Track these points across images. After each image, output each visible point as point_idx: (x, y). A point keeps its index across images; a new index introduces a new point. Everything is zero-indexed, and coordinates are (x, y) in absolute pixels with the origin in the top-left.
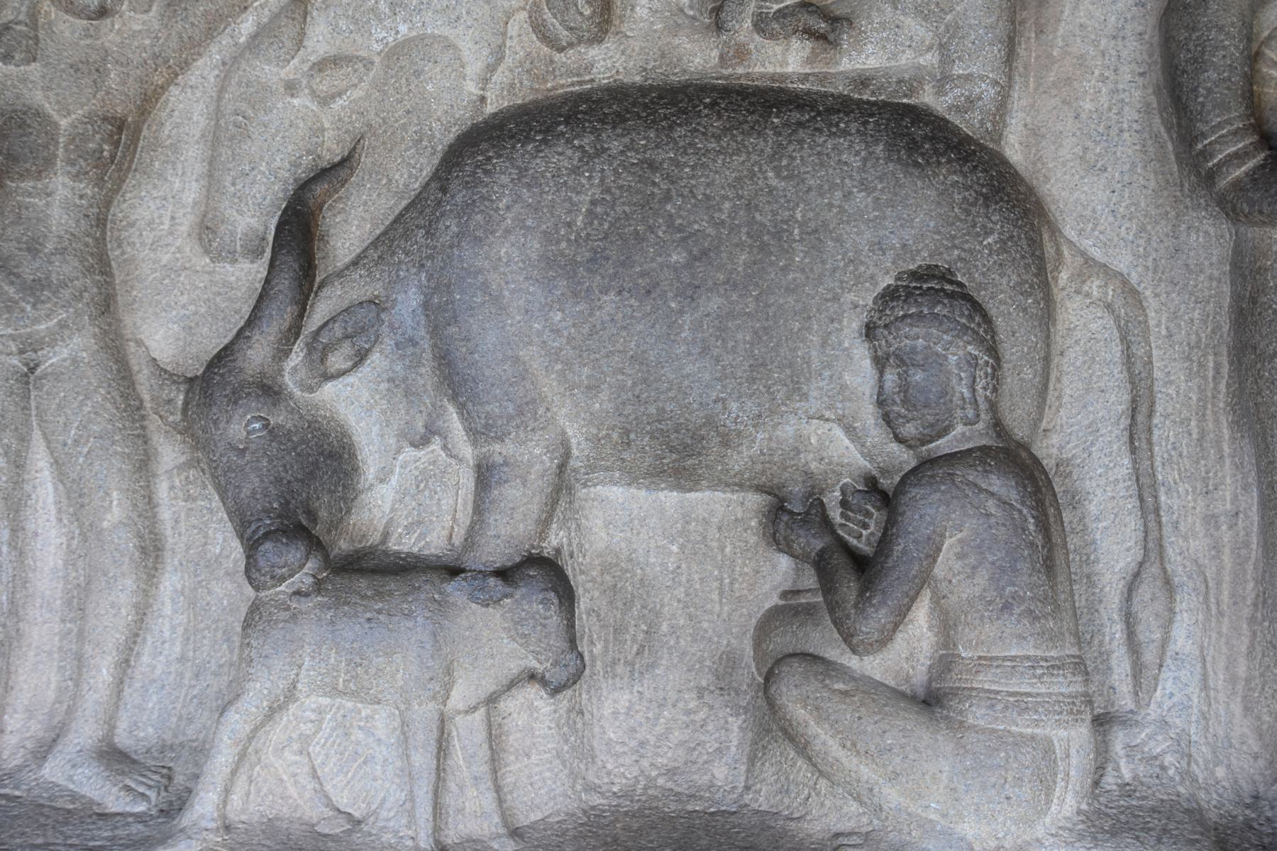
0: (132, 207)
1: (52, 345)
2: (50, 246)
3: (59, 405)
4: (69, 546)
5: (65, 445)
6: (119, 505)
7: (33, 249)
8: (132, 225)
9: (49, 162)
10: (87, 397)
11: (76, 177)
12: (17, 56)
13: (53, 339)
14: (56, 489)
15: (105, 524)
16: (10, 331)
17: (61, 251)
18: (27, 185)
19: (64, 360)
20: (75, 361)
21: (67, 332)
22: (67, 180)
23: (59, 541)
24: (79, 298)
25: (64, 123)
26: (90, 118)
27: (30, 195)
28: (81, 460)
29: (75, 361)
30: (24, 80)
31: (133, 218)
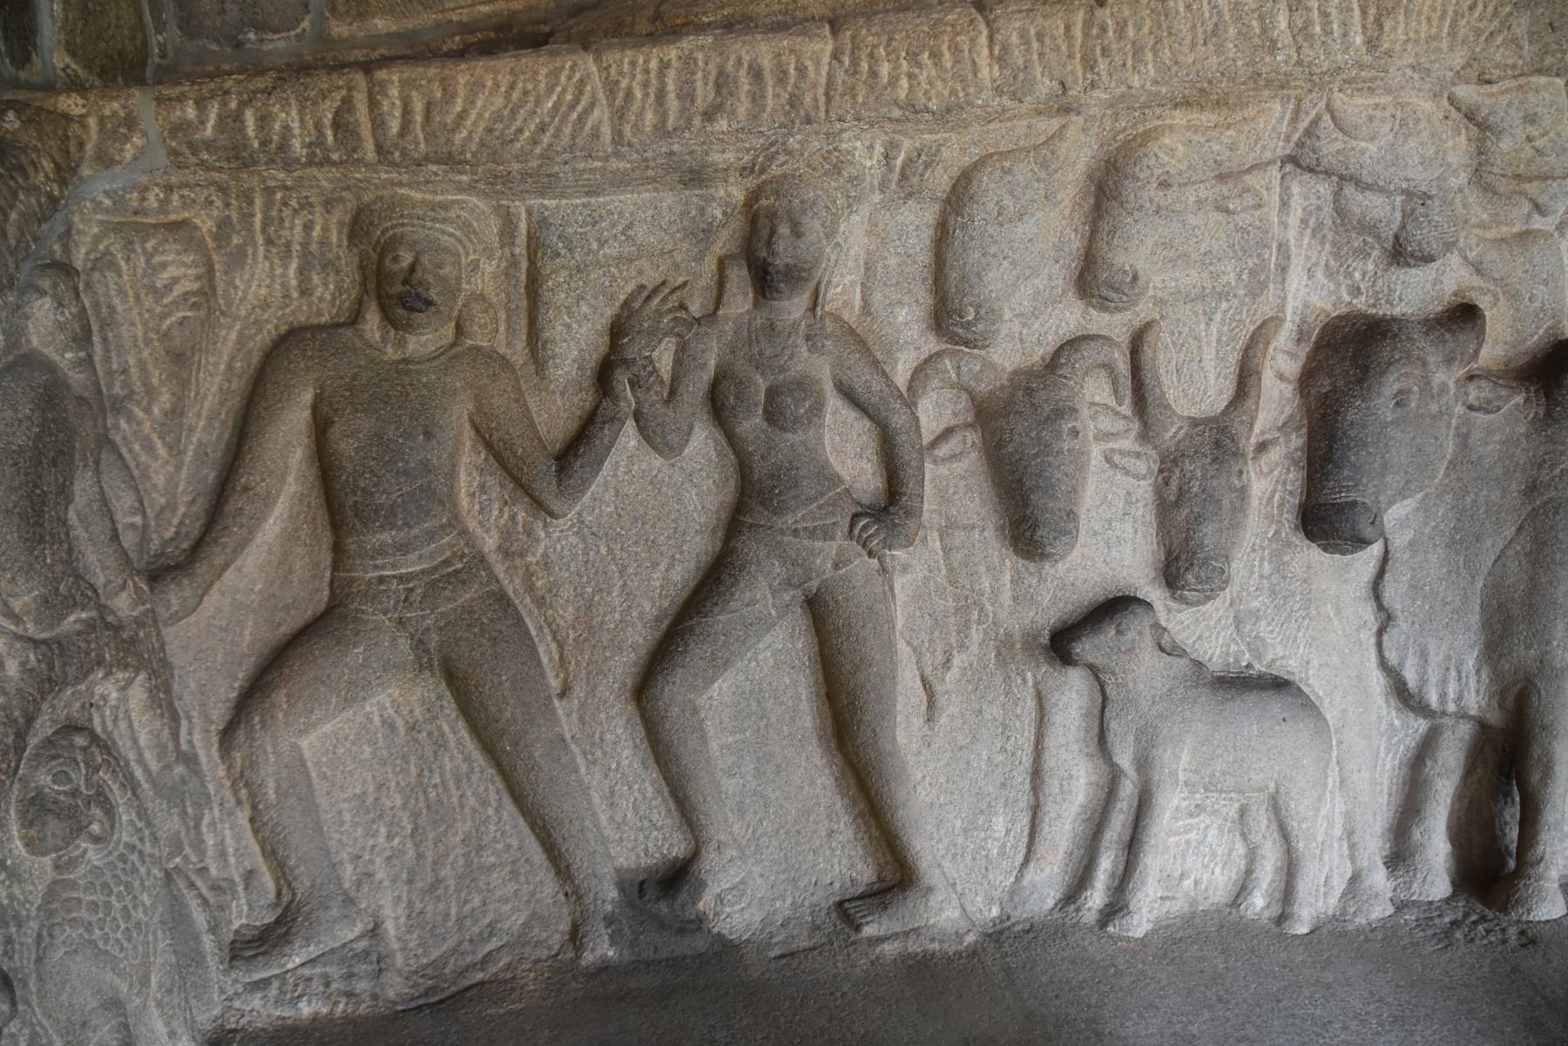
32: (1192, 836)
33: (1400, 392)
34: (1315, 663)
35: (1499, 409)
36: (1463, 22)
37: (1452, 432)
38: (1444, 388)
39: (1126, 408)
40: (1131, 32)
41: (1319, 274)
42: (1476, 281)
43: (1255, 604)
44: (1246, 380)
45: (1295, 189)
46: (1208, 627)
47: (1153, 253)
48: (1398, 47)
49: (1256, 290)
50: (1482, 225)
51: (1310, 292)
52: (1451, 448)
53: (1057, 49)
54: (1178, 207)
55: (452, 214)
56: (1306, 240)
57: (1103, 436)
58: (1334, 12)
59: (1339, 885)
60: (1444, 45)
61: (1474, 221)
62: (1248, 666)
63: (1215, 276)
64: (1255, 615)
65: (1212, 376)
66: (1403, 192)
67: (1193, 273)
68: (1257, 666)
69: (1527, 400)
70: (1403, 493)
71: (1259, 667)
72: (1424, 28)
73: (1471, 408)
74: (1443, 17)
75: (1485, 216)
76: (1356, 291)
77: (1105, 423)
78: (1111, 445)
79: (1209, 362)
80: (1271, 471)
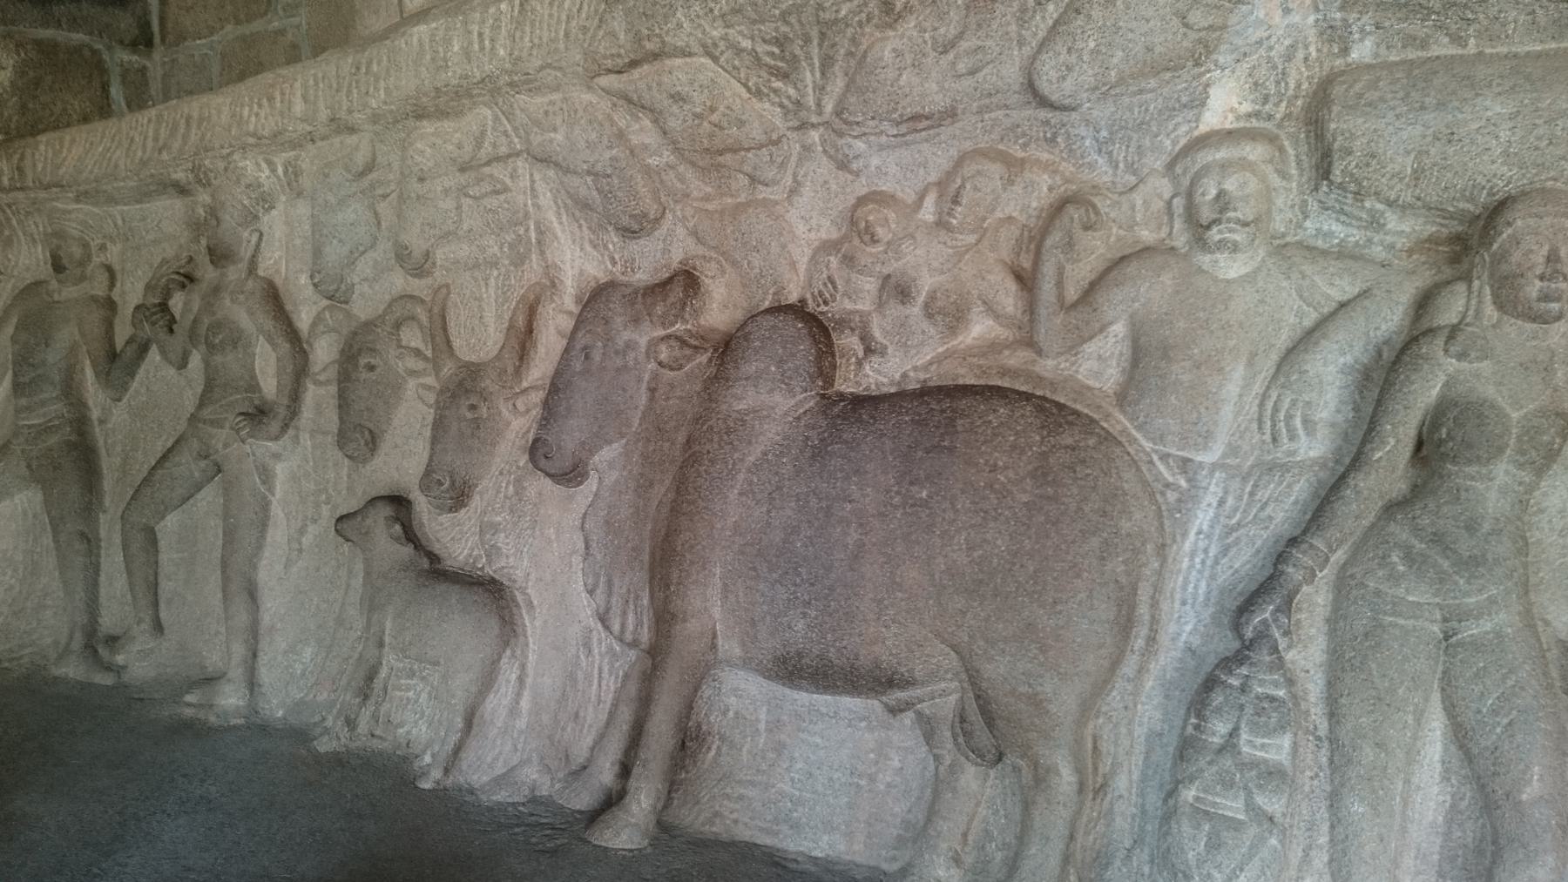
0: (1545, 494)
1: (1477, 618)
2: (1486, 527)
3: (1476, 675)
4: (1453, 806)
5: (1479, 712)
6: (1541, 779)
7: (1471, 527)
8: (1541, 511)
9: (1501, 450)
10: (1510, 671)
11: (1521, 466)
12: (1473, 355)
13: (1477, 614)
14: (1446, 750)
15: (1524, 797)
16: (1437, 600)
17: (1496, 532)
18: (1472, 470)
19: (1487, 633)
20: (1499, 635)
21: (1495, 608)
22: (1511, 467)
23: (1441, 798)
24: (1510, 577)
25: (1515, 415)
26: (1542, 412)
27: (1473, 478)
28: (1498, 730)
29: (1499, 635)
30: (1478, 376)
31: (1544, 505)
32: (411, 694)
33: (585, 348)
34: (533, 577)
35: (681, 367)
36: (574, 23)
37: (644, 386)
38: (630, 346)
39: (429, 353)
40: (375, 68)
41: (588, 248)
42: (701, 250)
43: (499, 519)
44: (523, 338)
45: (537, 177)
46: (461, 532)
47: (423, 231)
48: (525, 54)
49: (519, 260)
50: (707, 198)
51: (577, 260)
52: (643, 399)
53: (330, 87)
54: (430, 195)
55: (73, 216)
56: (564, 217)
57: (413, 373)
58: (487, 31)
59: (500, 769)
60: (562, 46)
61: (695, 194)
62: (482, 569)
63: (483, 249)
64: (495, 528)
65: (491, 330)
66: (589, 173)
67: (465, 247)
68: (487, 569)
69: (710, 360)
70: (598, 440)
71: (489, 571)
72: (546, 34)
73: (660, 364)
74: (559, 21)
75: (709, 189)
76: (614, 263)
77: (412, 363)
78: (421, 380)
79: (490, 316)
80: (528, 411)
